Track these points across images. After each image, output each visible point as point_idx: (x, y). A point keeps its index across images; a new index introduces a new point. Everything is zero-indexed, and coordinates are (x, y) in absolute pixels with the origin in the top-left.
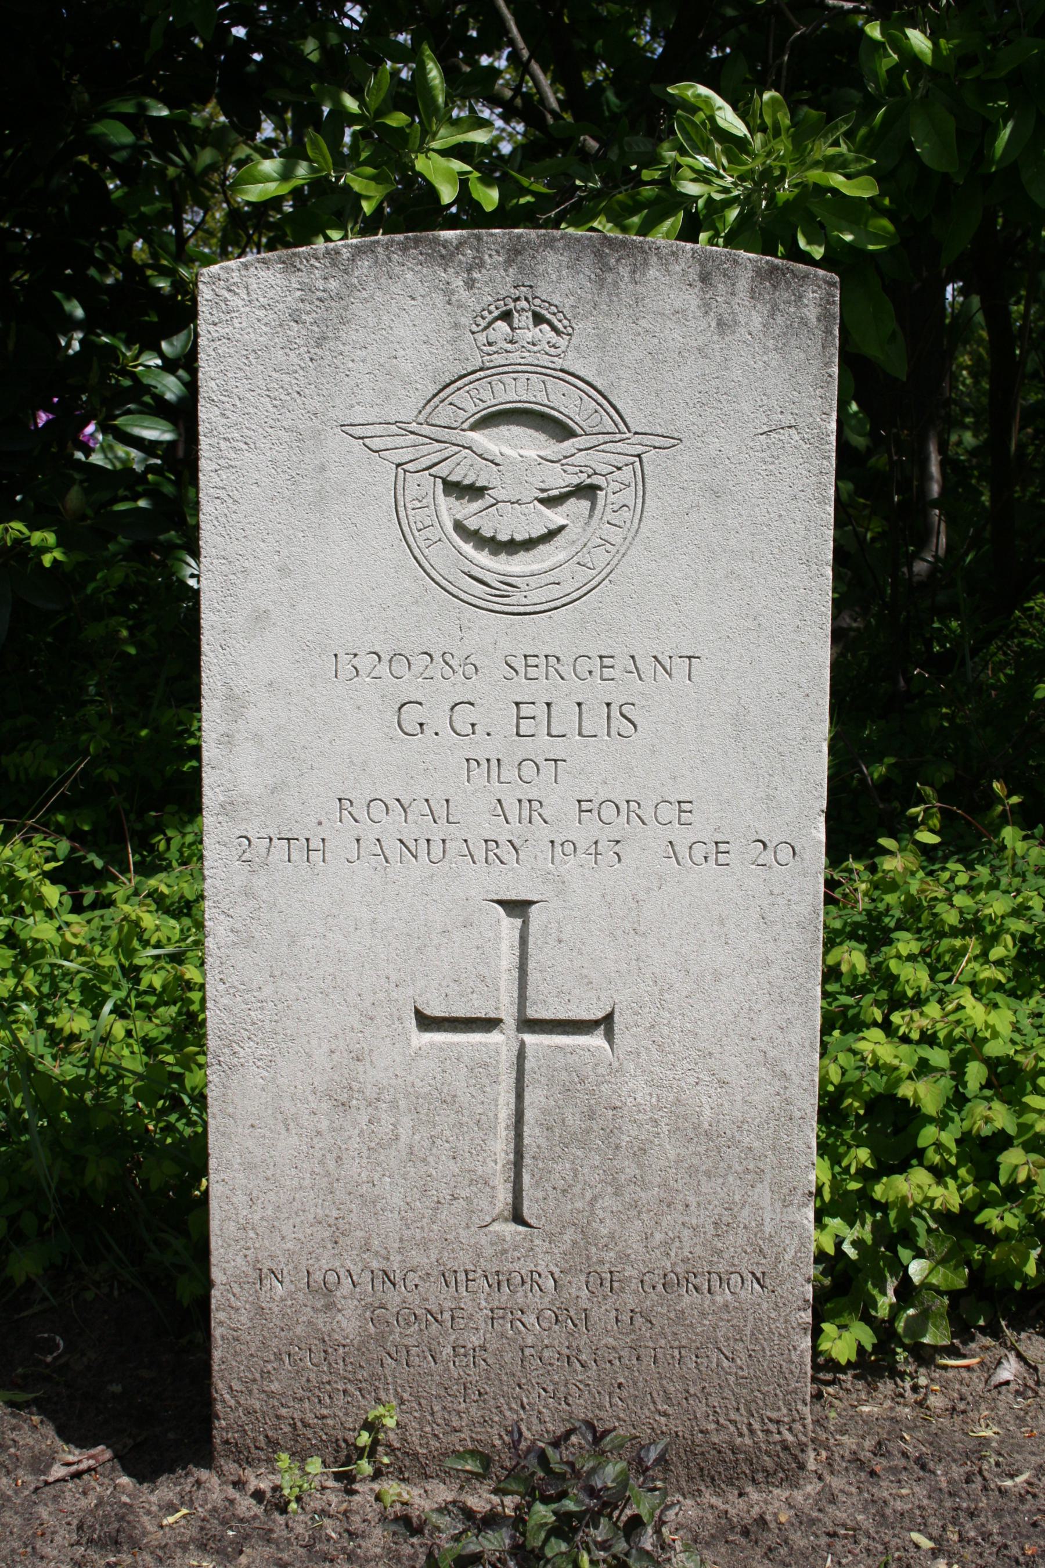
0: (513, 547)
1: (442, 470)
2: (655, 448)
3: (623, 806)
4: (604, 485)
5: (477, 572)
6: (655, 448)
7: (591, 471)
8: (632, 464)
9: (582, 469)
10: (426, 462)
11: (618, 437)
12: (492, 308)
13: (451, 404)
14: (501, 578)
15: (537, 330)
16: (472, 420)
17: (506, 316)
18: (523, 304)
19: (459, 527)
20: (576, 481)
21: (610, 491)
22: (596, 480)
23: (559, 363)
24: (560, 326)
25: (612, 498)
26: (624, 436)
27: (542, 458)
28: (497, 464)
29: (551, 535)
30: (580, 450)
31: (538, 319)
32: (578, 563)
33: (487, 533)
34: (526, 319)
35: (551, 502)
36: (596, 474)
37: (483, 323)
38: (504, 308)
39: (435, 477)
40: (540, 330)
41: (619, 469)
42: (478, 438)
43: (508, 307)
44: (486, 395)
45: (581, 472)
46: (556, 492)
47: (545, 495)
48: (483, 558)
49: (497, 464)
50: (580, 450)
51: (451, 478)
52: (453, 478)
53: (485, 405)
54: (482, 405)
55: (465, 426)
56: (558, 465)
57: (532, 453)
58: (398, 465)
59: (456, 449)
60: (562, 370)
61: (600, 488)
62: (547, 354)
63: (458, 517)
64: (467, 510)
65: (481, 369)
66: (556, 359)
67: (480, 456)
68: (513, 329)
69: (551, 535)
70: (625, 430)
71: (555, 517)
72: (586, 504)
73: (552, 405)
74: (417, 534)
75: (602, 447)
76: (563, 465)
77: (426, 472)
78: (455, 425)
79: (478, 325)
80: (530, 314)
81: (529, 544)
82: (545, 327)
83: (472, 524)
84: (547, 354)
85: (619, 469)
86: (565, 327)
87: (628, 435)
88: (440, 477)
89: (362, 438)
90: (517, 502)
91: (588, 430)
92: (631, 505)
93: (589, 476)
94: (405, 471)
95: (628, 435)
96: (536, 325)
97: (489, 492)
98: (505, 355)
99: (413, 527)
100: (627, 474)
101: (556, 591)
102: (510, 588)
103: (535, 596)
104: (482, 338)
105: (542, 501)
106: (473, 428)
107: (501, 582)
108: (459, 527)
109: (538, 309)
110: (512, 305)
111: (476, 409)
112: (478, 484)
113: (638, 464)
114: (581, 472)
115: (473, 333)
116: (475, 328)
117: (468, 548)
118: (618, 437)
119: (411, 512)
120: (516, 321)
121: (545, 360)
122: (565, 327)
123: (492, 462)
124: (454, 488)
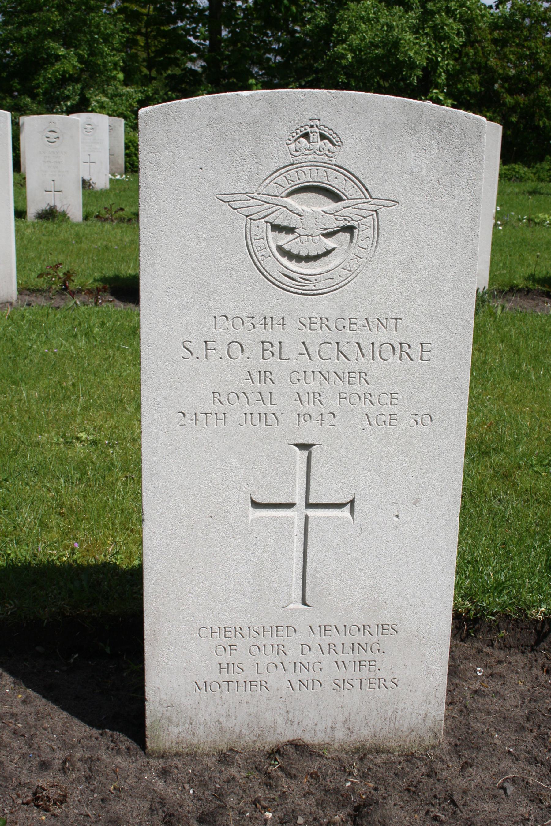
0: (308, 259)
2: (384, 206)
3: (362, 396)
4: (357, 226)
6: (384, 206)
7: (350, 219)
8: (372, 215)
11: (365, 200)
12: (298, 131)
13: (276, 183)
15: (322, 143)
17: (306, 136)
18: (315, 129)
19: (280, 249)
20: (342, 224)
21: (360, 229)
23: (334, 161)
24: (334, 141)
25: (361, 233)
26: (367, 200)
27: (324, 212)
28: (300, 216)
29: (328, 252)
31: (323, 137)
32: (343, 268)
33: (295, 251)
34: (315, 137)
35: (329, 235)
36: (353, 220)
37: (293, 139)
38: (304, 132)
39: (267, 222)
40: (324, 143)
41: (365, 218)
42: (290, 201)
44: (295, 178)
45: (345, 219)
46: (332, 230)
47: (326, 231)
48: (292, 265)
49: (300, 216)
50: (344, 208)
52: (277, 222)
53: (294, 183)
54: (293, 183)
55: (283, 195)
56: (332, 216)
57: (319, 209)
58: (247, 216)
59: (277, 207)
60: (335, 165)
61: (354, 228)
62: (327, 156)
63: (280, 244)
64: (285, 240)
65: (292, 164)
66: (331, 159)
67: (291, 211)
68: (310, 143)
69: (328, 252)
70: (368, 196)
71: (330, 243)
72: (347, 235)
74: (257, 253)
75: (356, 206)
76: (335, 215)
77: (263, 220)
78: (277, 194)
79: (290, 140)
80: (318, 134)
81: (317, 257)
82: (326, 141)
83: (287, 247)
84: (327, 156)
85: (365, 218)
86: (337, 142)
88: (269, 222)
89: (228, 202)
90: (310, 236)
91: (350, 197)
93: (349, 222)
94: (251, 219)
95: (370, 200)
96: (321, 140)
97: (296, 230)
98: (305, 156)
99: (255, 248)
101: (332, 282)
104: (293, 147)
105: (324, 235)
107: (301, 278)
108: (280, 249)
109: (323, 132)
110: (309, 130)
113: (375, 215)
114: (345, 219)
115: (287, 145)
116: (289, 142)
117: (284, 261)
119: (254, 242)
120: (311, 138)
121: (326, 159)
122: (337, 142)
123: (297, 214)
124: (276, 228)
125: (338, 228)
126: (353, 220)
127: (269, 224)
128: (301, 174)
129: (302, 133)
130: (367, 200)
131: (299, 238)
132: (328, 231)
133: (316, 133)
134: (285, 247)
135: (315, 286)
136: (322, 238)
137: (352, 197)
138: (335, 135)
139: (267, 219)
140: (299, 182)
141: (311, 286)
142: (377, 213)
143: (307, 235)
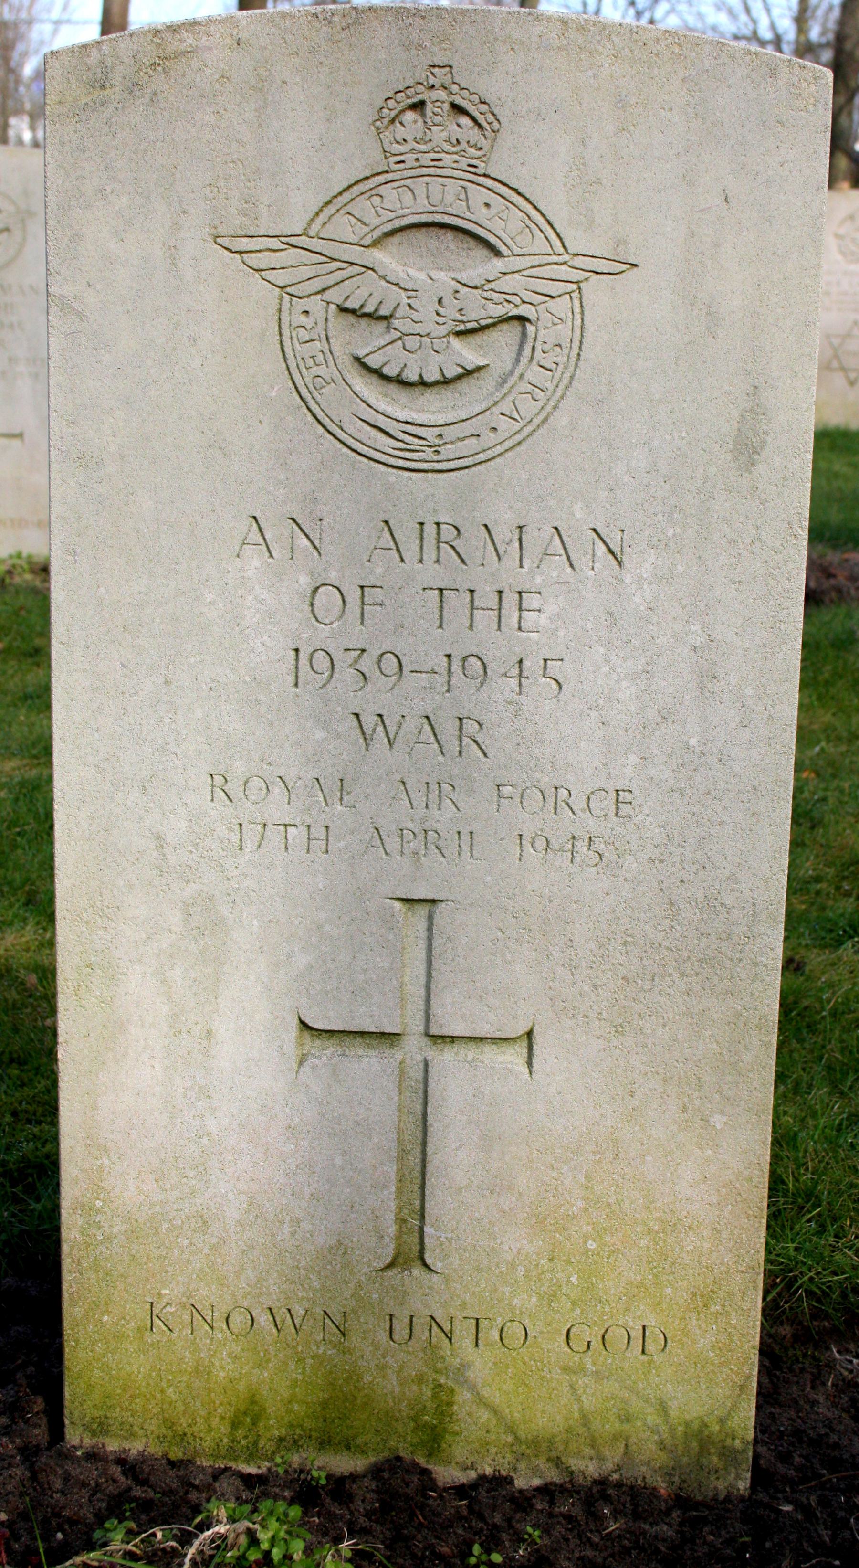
1: (335, 296)
5: (382, 421)
9: (508, 297)
10: (317, 284)
14: (409, 428)
16: (377, 234)
17: (419, 106)
20: (499, 311)
22: (524, 310)
30: (504, 274)
36: (524, 302)
42: (380, 257)
43: (420, 97)
45: (509, 302)
46: (474, 325)
47: (462, 327)
51: (348, 305)
55: (367, 241)
58: (282, 288)
65: (387, 172)
67: (384, 278)
70: (562, 250)
73: (473, 217)
77: (319, 297)
80: (446, 106)
82: (465, 121)
83: (374, 361)
87: (566, 257)
91: (517, 251)
92: (566, 344)
95: (566, 257)
100: (561, 306)
102: (416, 441)
103: (448, 451)
105: (458, 334)
106: (376, 243)
109: (458, 101)
111: (376, 221)
112: (383, 312)
113: (575, 295)
114: (509, 302)
118: (555, 258)
125: (490, 321)
126: (524, 302)
127: (333, 307)
128: (408, 196)
129: (410, 101)
130: (555, 258)
131: (400, 342)
132: (470, 326)
133: (443, 102)
134: (368, 361)
135: (438, 452)
136: (455, 342)
137: (525, 251)
138: (484, 108)
139: (327, 296)
140: (401, 212)
141: (429, 454)
142: (579, 288)
143: (418, 334)
